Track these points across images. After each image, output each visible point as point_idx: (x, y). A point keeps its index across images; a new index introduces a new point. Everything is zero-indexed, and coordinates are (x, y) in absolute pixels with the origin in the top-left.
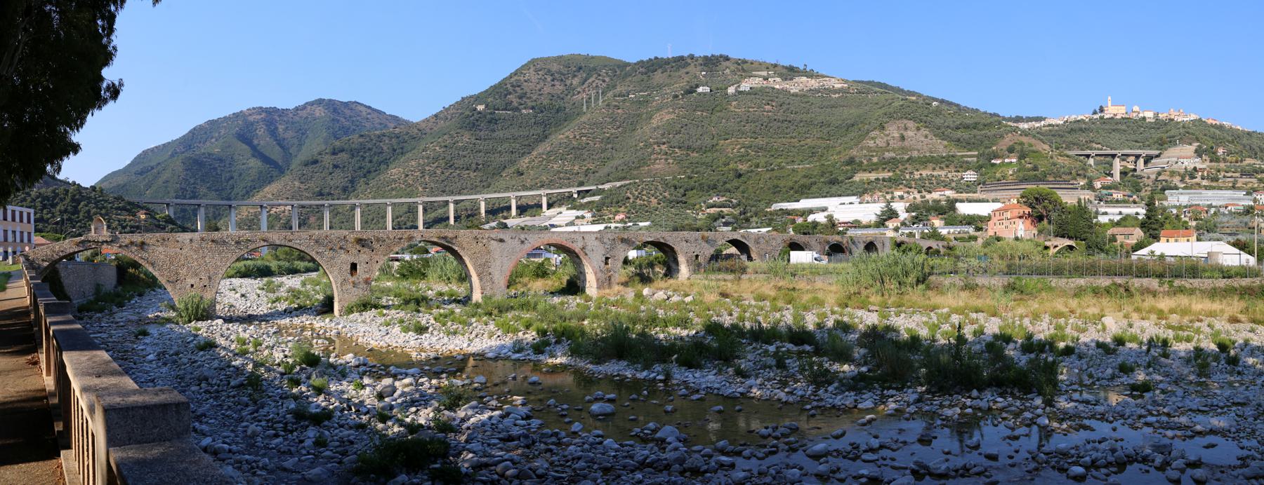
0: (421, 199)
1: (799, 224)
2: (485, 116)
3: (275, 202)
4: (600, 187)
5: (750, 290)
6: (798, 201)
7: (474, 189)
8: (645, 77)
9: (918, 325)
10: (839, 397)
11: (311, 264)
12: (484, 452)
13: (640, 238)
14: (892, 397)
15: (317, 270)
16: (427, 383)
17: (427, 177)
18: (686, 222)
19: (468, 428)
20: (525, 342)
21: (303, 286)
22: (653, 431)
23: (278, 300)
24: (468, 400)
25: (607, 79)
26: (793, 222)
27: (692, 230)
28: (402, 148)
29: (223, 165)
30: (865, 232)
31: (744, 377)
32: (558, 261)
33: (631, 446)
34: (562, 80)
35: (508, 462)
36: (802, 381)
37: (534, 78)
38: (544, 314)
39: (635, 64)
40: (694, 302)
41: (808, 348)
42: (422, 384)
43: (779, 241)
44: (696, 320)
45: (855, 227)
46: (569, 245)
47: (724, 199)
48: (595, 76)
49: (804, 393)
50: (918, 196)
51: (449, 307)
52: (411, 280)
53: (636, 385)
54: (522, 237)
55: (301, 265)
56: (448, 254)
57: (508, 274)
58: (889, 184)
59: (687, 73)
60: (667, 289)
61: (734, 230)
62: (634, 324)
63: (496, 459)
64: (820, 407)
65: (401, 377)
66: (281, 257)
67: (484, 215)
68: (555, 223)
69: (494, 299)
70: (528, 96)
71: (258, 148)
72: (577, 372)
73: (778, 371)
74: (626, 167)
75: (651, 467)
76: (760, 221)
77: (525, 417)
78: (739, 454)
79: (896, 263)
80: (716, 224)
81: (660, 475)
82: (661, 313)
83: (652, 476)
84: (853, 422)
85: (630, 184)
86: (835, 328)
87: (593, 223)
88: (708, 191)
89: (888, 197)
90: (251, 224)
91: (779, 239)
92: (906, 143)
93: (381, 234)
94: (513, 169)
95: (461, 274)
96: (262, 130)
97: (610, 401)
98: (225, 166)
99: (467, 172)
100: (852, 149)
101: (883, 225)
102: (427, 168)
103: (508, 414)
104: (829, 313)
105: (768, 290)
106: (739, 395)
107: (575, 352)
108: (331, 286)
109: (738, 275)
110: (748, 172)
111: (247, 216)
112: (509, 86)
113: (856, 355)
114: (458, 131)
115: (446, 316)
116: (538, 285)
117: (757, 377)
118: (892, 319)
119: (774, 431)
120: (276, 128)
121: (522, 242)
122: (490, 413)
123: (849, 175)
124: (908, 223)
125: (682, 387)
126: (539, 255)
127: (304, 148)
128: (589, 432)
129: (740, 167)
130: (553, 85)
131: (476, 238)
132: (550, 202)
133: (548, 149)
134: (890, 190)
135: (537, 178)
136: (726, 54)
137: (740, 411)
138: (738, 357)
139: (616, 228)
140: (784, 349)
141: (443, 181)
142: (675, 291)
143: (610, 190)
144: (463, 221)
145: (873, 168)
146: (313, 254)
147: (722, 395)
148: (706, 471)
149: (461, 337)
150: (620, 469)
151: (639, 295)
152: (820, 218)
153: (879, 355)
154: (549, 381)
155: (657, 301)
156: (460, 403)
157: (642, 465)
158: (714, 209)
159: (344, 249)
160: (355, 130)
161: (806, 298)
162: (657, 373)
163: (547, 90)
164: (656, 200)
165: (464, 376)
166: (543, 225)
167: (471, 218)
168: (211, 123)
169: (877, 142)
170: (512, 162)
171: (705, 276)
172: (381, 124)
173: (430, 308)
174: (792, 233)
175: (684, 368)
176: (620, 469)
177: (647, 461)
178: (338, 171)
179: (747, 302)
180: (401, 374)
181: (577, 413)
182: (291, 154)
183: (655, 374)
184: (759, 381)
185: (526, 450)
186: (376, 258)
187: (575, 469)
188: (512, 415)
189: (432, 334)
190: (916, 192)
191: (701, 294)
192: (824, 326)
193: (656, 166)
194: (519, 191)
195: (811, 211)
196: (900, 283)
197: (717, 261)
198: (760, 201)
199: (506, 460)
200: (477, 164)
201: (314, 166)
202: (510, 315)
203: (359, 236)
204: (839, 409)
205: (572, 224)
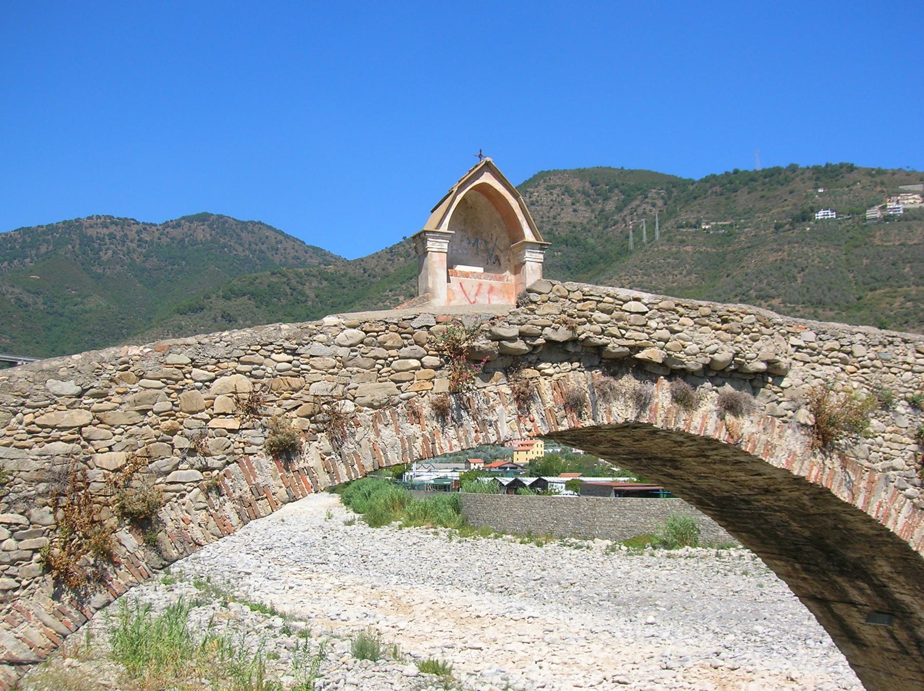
8: (722, 199)
39: (702, 181)
59: (791, 192)
130: (575, 211)
136: (850, 162)
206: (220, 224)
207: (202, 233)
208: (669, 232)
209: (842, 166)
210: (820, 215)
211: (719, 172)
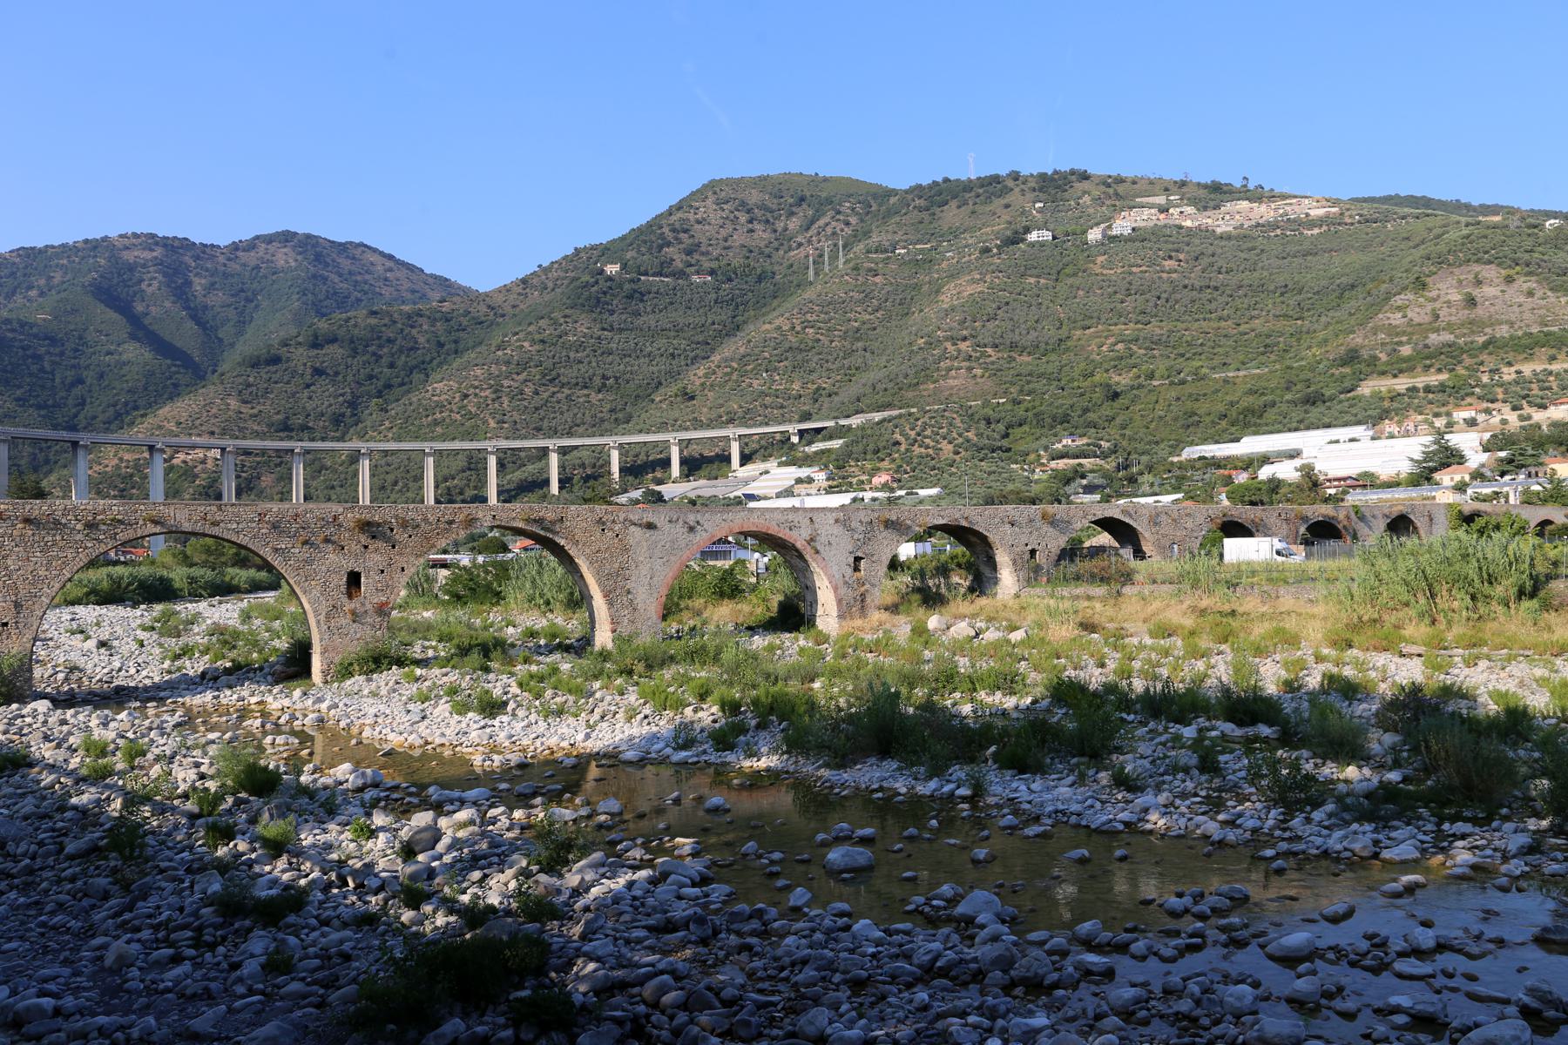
0: (494, 443)
1: (1240, 485)
2: (620, 286)
3: (184, 440)
4: (842, 422)
5: (1142, 616)
6: (1237, 440)
7: (598, 426)
8: (925, 215)
9: (1521, 684)
10: (1338, 834)
11: (263, 575)
12: (617, 958)
13: (920, 520)
14: (1463, 837)
15: (274, 586)
16: (503, 818)
17: (506, 400)
18: (1010, 487)
19: (587, 909)
20: (697, 727)
21: (243, 622)
22: (948, 901)
23: (186, 651)
24: (585, 851)
25: (853, 220)
26: (1228, 481)
27: (1023, 501)
28: (456, 342)
29: (57, 350)
30: (1386, 495)
31: (1130, 789)
32: (761, 565)
33: (907, 933)
34: (767, 221)
35: (665, 977)
36: (1254, 798)
37: (715, 217)
38: (735, 669)
40: (1028, 642)
41: (1265, 730)
42: (494, 821)
43: (1200, 519)
44: (1033, 676)
45: (1364, 486)
46: (783, 533)
47: (1085, 441)
48: (831, 213)
49: (1258, 823)
50: (1512, 418)
51: (548, 660)
52: (471, 606)
53: (915, 808)
54: (691, 518)
55: (241, 575)
56: (546, 553)
57: (665, 592)
58: (1440, 396)
60: (974, 616)
61: (1106, 499)
62: (912, 686)
63: (643, 970)
64: (1295, 854)
65: (451, 808)
66: (196, 560)
67: (616, 476)
68: (755, 492)
69: (639, 641)
70: (703, 249)
71: (146, 322)
72: (801, 786)
73: (1203, 778)
74: (892, 385)
75: (945, 976)
76: (1157, 481)
77: (698, 879)
78: (1123, 948)
79: (1465, 556)
80: (1069, 489)
81: (963, 993)
82: (963, 663)
83: (948, 996)
84: (1371, 889)
85: (900, 416)
86: (1324, 691)
87: (830, 490)
88: (1052, 427)
89: (1440, 423)
90: (128, 485)
91: (1201, 517)
93: (411, 512)
94: (674, 389)
95: (572, 594)
96: (155, 284)
97: (866, 841)
98: (62, 354)
99: (585, 392)
100: (1354, 332)
101: (1429, 479)
102: (506, 383)
103: (664, 876)
104: (1311, 659)
105: (1178, 614)
106: (1121, 827)
107: (795, 744)
108: (305, 621)
109: (1115, 587)
110: (1132, 388)
111: (118, 467)
112: (666, 230)
113: (1375, 747)
114: (568, 312)
115: (541, 679)
116: (723, 614)
117: (1158, 789)
118: (1456, 671)
119: (1196, 903)
120: (189, 283)
121: (691, 529)
122: (629, 876)
123: (1347, 384)
124: (1489, 474)
125: (1006, 811)
126: (725, 555)
127: (250, 331)
128: (824, 906)
129: (1117, 379)
130: (752, 231)
131: (600, 521)
132: (747, 451)
133: (742, 350)
134: (1443, 410)
135: (721, 406)
137: (1123, 859)
138: (1119, 750)
139: (874, 499)
140: (1214, 733)
141: (537, 409)
142: (990, 619)
143: (862, 428)
144: (576, 488)
145: (1400, 367)
146: (267, 553)
147: (1087, 827)
148: (1056, 985)
149: (571, 720)
150: (884, 983)
151: (920, 631)
152: (1286, 471)
153: (1427, 747)
154: (747, 804)
155: (955, 641)
156: (571, 856)
157: (929, 972)
158: (1066, 461)
159: (333, 543)
160: (359, 300)
161: (1259, 630)
162: (956, 782)
163: (739, 239)
164: (950, 447)
165: (578, 801)
166: (732, 496)
167: (591, 483)
168: (29, 254)
169: (1410, 314)
170: (674, 375)
171: (1049, 589)
172: (413, 292)
173: (511, 662)
174: (1226, 503)
175: (1010, 772)
176: (884, 983)
177: (939, 964)
178: (323, 381)
179: (1135, 641)
180: (451, 802)
181: (802, 868)
182: (221, 340)
183: (952, 786)
184: (1163, 798)
185: (700, 949)
186: (401, 561)
187: (796, 983)
188: (673, 877)
189: (514, 715)
190: (1506, 409)
191: (1041, 626)
192: (1300, 687)
193: (951, 382)
194: (687, 429)
195: (1265, 459)
196: (1473, 598)
197: (1072, 561)
198: (1157, 443)
199: (662, 972)
200: (604, 377)
201: (273, 368)
202: (667, 673)
203: (366, 516)
204: (1338, 860)
205: (788, 493)
206: (309, 245)
207: (284, 258)
208: (857, 257)
209: (1073, 172)
210: (1033, 236)
211: (926, 182)
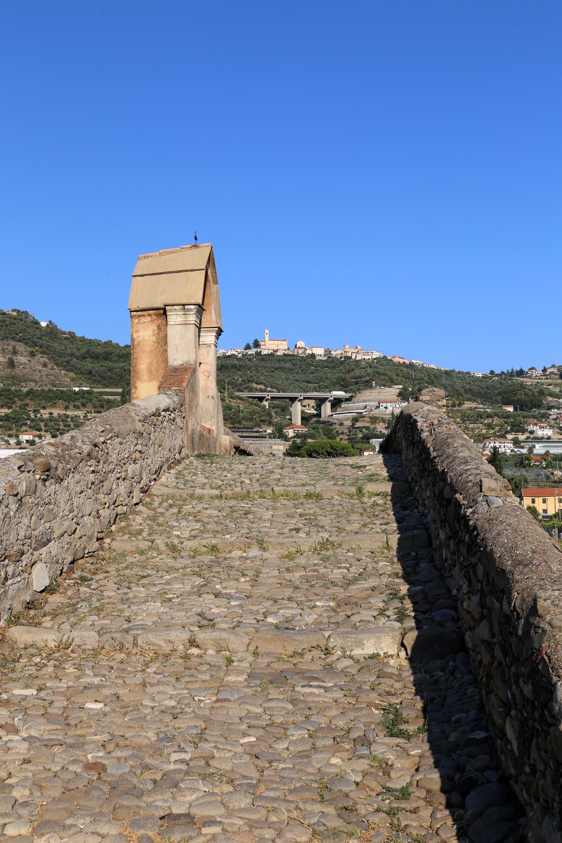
58: (6, 423)
92: (17, 371)
190: (49, 436)
